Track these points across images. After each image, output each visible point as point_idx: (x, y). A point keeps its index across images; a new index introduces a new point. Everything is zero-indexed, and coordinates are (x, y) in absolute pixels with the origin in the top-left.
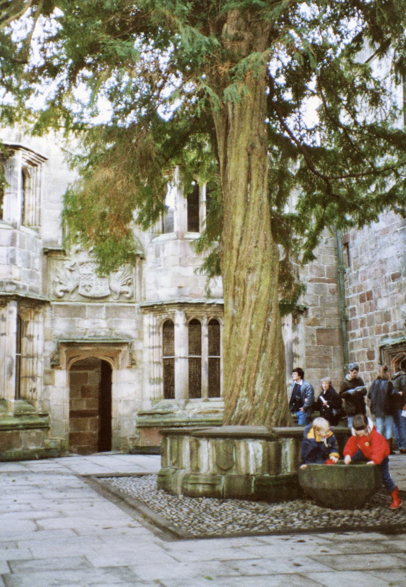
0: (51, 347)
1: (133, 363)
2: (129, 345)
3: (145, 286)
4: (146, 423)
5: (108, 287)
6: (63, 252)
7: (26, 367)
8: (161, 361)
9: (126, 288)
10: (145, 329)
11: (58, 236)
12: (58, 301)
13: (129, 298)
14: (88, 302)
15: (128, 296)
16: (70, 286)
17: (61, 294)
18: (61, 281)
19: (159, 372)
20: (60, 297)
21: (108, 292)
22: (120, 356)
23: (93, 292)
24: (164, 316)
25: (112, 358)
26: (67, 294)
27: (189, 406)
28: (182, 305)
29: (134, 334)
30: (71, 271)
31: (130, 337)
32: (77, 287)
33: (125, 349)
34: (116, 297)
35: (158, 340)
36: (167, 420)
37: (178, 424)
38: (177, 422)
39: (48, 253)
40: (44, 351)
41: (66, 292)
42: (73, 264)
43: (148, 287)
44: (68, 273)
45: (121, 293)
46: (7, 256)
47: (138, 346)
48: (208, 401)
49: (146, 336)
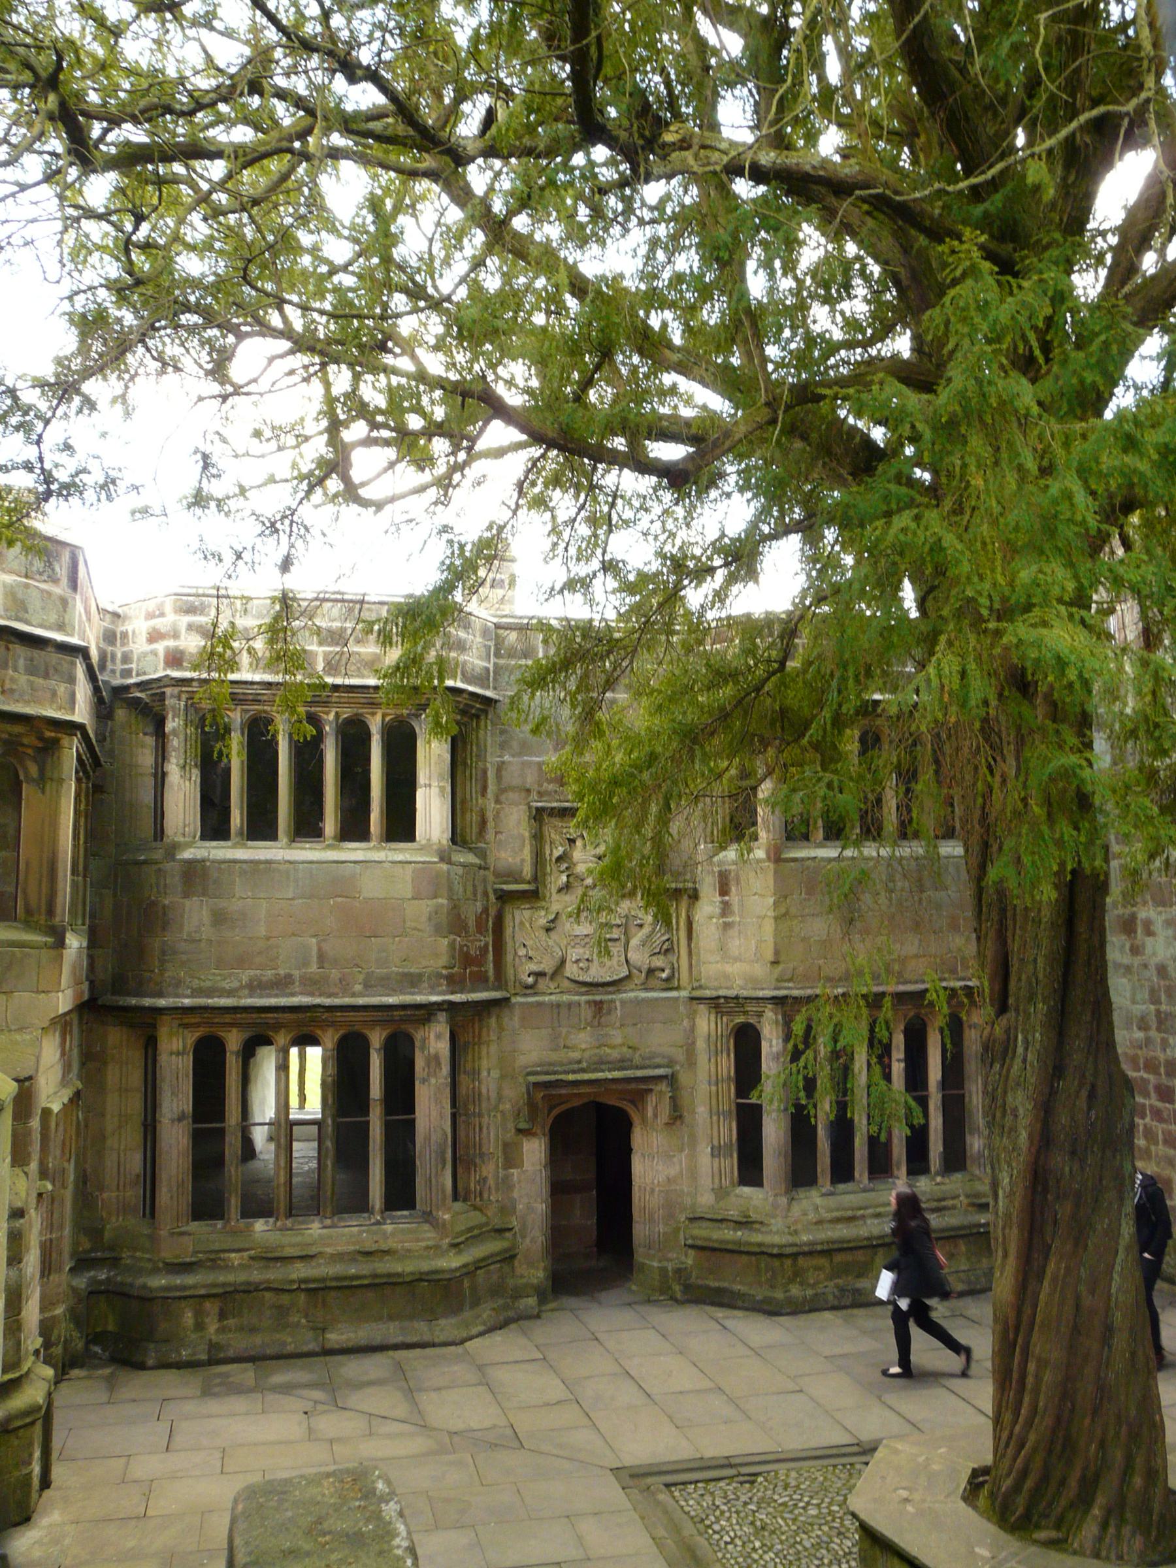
0: (514, 1093)
1: (677, 1116)
2: (672, 1080)
3: (699, 954)
4: (710, 1240)
5: (623, 958)
6: (533, 896)
7: (467, 1136)
8: (733, 1107)
9: (658, 962)
10: (701, 1044)
11: (523, 861)
12: (525, 995)
13: (667, 980)
14: (582, 994)
15: (664, 975)
16: (547, 965)
17: (531, 980)
18: (531, 953)
19: (729, 1131)
20: (527, 987)
21: (624, 972)
22: (651, 1100)
23: (597, 973)
24: (741, 1019)
25: (633, 1102)
26: (540, 980)
27: (796, 1210)
28: (779, 1001)
29: (680, 1056)
30: (548, 930)
31: (671, 1063)
32: (563, 962)
33: (663, 1087)
34: (639, 978)
35: (727, 1065)
36: (757, 1238)
37: (775, 1251)
38: (773, 1246)
39: (505, 897)
40: (500, 1098)
41: (539, 975)
42: (552, 917)
43: (704, 956)
44: (542, 933)
45: (651, 971)
46: (430, 919)
47: (684, 1078)
48: (832, 1194)
49: (702, 1058)
